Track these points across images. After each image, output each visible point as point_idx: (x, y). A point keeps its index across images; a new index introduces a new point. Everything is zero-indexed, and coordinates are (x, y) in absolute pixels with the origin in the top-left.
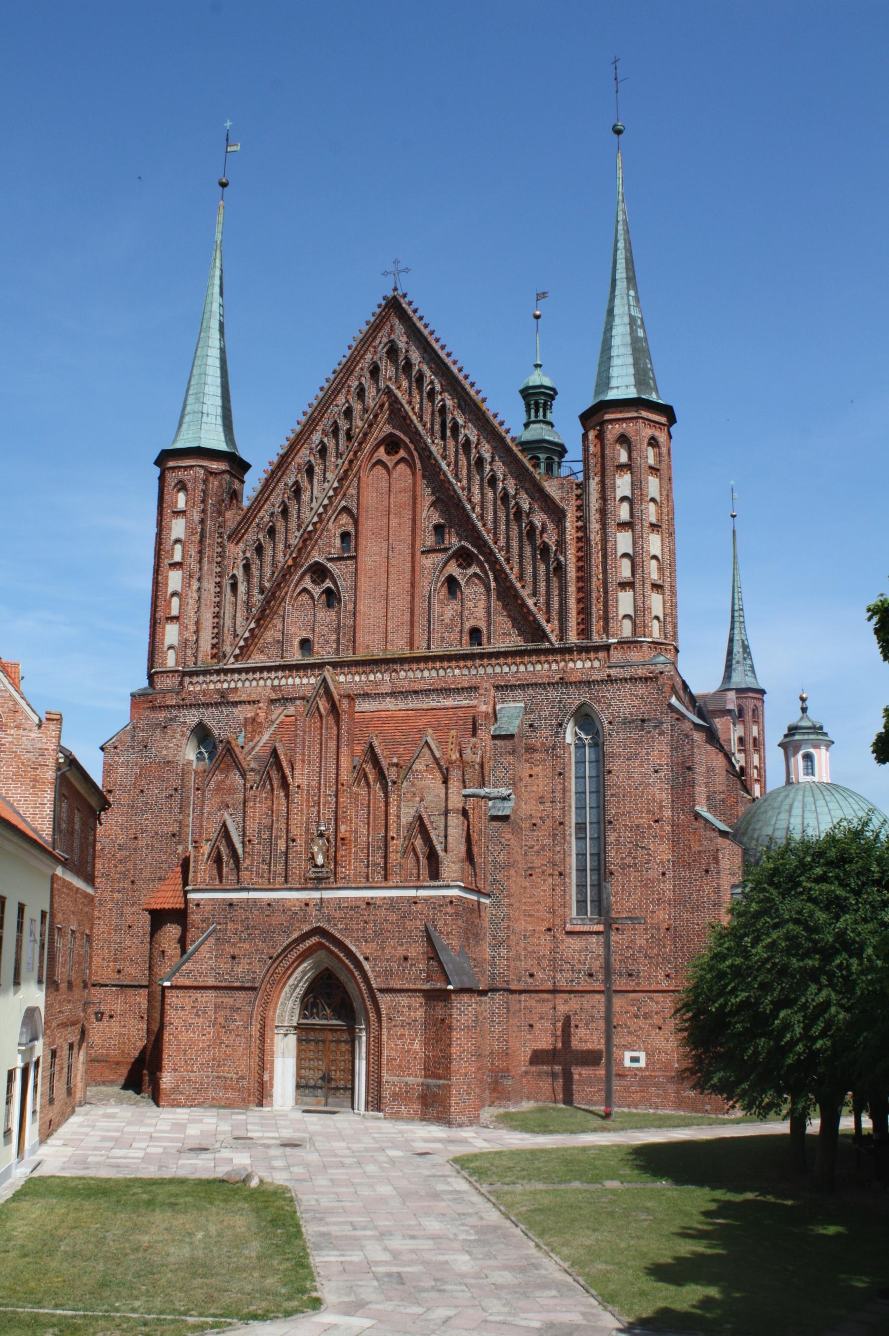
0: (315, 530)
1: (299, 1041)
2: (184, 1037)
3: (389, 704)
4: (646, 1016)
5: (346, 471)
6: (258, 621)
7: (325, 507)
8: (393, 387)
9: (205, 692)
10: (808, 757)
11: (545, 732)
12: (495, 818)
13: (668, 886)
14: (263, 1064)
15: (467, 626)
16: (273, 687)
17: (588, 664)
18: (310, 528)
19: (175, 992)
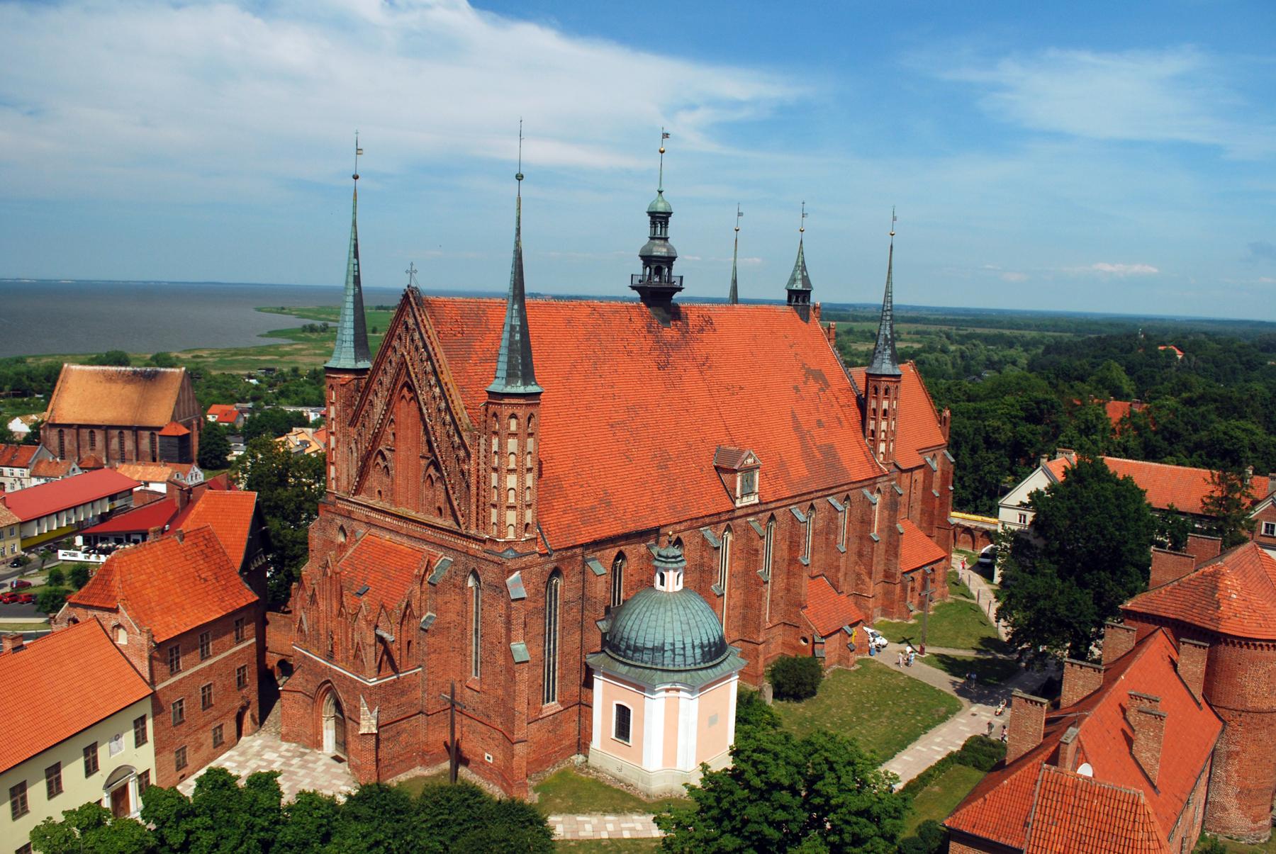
0: (379, 432)
1: (336, 722)
2: (290, 712)
3: (405, 540)
4: (493, 739)
5: (389, 400)
6: (360, 477)
7: (382, 420)
8: (406, 354)
9: (343, 509)
10: (662, 576)
11: (460, 579)
12: (422, 629)
13: (502, 678)
14: (318, 732)
15: (437, 505)
16: (366, 515)
17: (477, 547)
18: (376, 431)
19: (285, 692)
